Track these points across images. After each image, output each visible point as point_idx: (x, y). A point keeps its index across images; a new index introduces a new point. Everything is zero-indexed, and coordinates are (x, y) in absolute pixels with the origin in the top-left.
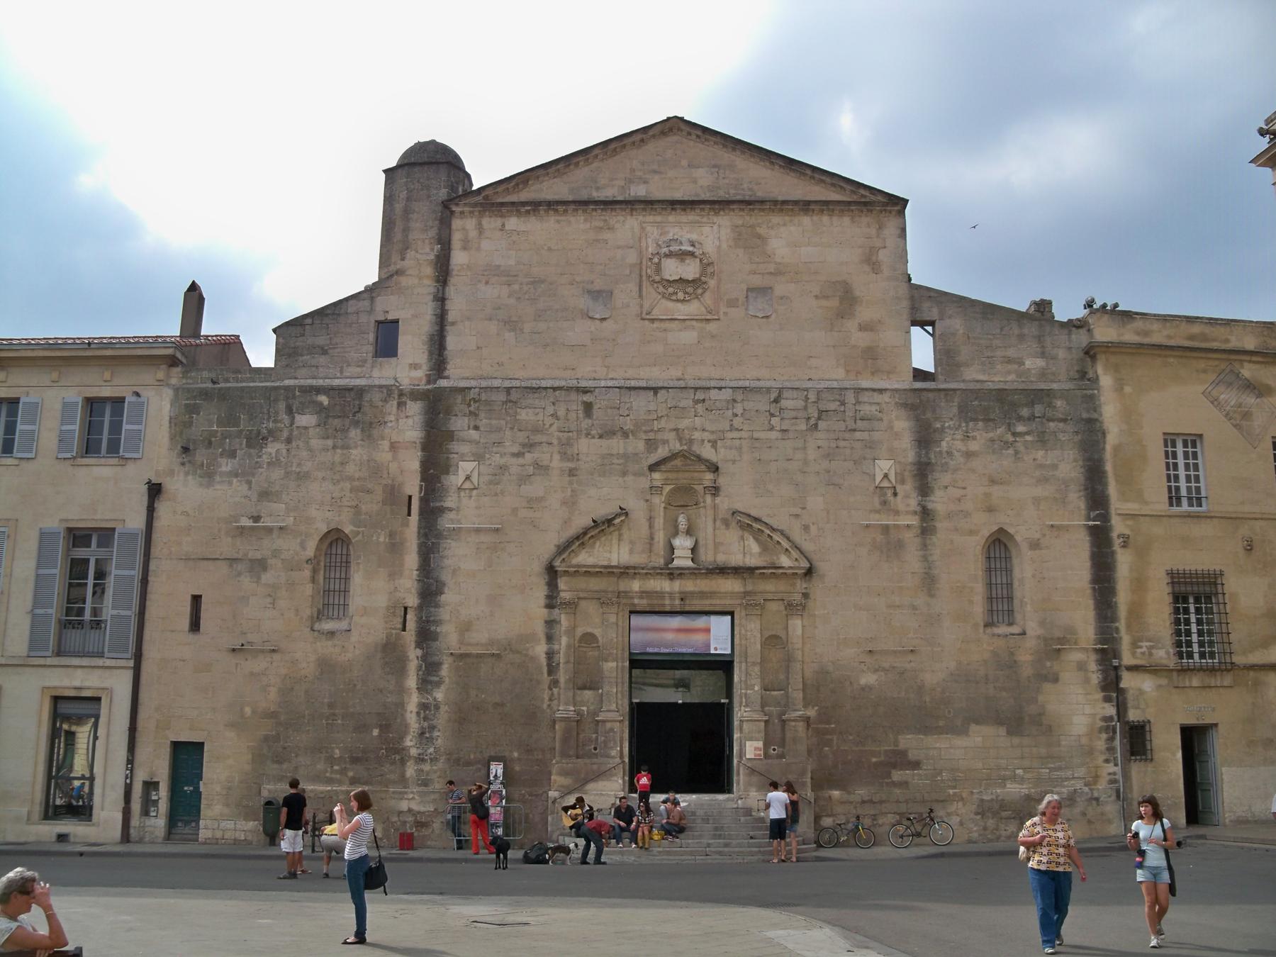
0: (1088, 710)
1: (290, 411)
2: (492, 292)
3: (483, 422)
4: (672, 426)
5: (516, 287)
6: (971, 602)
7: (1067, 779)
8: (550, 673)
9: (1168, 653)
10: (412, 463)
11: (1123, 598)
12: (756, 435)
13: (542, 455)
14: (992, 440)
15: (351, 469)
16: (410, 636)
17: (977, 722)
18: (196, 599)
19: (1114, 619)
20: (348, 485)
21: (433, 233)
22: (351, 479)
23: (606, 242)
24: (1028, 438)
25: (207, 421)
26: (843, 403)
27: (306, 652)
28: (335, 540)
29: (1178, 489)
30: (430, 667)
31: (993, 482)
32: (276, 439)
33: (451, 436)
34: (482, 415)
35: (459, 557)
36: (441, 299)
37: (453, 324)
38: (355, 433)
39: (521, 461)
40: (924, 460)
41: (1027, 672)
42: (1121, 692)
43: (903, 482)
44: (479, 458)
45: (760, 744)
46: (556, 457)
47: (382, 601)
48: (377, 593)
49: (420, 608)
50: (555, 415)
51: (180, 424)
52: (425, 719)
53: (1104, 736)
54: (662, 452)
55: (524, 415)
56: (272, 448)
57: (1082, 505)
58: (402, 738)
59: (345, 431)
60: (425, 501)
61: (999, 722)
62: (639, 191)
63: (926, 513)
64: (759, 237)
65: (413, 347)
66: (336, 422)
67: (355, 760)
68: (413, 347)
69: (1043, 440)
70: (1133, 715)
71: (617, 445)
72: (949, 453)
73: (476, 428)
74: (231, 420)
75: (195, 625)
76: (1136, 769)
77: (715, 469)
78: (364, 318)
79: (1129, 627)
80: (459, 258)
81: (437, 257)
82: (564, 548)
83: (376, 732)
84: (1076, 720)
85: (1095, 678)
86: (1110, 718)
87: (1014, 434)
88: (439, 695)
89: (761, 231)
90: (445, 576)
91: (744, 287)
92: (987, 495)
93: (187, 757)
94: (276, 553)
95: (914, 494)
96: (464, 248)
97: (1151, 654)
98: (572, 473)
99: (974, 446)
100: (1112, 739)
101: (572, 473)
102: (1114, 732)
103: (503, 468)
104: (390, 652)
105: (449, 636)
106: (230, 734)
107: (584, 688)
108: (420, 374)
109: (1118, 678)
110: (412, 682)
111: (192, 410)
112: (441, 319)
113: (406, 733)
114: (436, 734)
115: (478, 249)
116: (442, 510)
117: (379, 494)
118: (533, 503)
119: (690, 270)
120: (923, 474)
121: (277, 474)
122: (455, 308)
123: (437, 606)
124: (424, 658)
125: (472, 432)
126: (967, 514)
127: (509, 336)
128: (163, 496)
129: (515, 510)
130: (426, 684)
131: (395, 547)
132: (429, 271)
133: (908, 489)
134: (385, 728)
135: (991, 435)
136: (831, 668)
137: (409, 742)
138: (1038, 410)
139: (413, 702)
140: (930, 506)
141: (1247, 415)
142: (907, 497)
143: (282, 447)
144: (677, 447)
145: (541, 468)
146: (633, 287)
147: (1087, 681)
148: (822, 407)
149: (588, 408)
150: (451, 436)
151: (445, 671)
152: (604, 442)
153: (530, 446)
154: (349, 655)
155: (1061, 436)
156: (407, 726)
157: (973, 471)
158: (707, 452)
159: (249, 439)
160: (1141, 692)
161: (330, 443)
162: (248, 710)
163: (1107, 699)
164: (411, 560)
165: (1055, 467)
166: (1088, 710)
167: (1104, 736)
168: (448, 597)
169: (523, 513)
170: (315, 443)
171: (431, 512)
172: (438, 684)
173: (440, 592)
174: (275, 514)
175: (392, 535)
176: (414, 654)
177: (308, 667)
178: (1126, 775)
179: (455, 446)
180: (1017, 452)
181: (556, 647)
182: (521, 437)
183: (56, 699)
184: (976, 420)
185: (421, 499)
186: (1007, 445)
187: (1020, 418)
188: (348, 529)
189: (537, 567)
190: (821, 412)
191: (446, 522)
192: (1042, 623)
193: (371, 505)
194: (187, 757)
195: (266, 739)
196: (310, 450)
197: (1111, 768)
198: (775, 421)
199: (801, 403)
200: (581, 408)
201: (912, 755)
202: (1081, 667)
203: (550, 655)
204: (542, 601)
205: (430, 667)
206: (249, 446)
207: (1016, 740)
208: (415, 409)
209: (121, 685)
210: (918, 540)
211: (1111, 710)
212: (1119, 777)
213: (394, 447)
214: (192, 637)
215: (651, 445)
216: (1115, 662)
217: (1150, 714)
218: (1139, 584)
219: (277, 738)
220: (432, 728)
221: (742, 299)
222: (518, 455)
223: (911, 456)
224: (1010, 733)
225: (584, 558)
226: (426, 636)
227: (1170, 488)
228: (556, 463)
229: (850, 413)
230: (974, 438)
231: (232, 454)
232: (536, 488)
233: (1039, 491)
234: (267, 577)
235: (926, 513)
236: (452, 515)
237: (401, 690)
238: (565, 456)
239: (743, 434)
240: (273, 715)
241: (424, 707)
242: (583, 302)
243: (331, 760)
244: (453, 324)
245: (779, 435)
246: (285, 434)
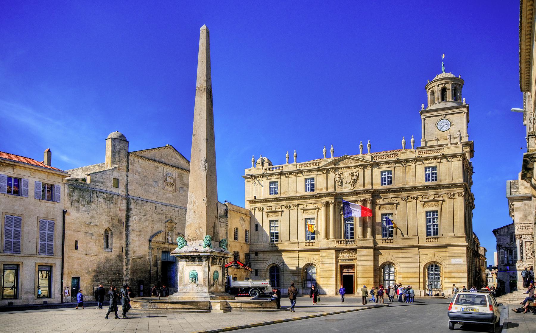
2: (136, 177)
10: (124, 214)
13: (148, 217)
16: (124, 254)
18: (77, 242)
20: (111, 217)
21: (126, 159)
25: (76, 195)
27: (103, 255)
28: (108, 230)
30: (128, 261)
35: (133, 236)
38: (112, 205)
44: (136, 215)
47: (118, 245)
48: (116, 243)
54: (167, 219)
55: (145, 207)
60: (127, 223)
62: (163, 160)
65: (122, 187)
66: (108, 202)
67: (113, 281)
68: (122, 187)
71: (160, 216)
77: (176, 224)
78: (111, 177)
80: (130, 167)
82: (152, 236)
88: (129, 266)
90: (130, 241)
93: (76, 280)
98: (153, 221)
101: (153, 221)
104: (120, 257)
106: (87, 275)
108: (124, 193)
110: (124, 264)
119: (172, 181)
124: (127, 258)
127: (140, 188)
128: (66, 214)
130: (127, 264)
131: (121, 233)
134: (119, 274)
137: (124, 277)
139: (125, 269)
143: (96, 206)
144: (170, 218)
146: (162, 182)
150: (131, 209)
151: (130, 262)
158: (174, 220)
161: (106, 207)
162: (90, 269)
164: (124, 236)
168: (131, 246)
170: (104, 206)
171: (127, 226)
174: (94, 222)
175: (120, 230)
176: (125, 257)
177: (103, 260)
179: (131, 212)
188: (111, 228)
189: (147, 241)
191: (130, 228)
193: (116, 222)
194: (76, 280)
195: (94, 276)
205: (128, 261)
206: (88, 204)
208: (124, 201)
209: (58, 262)
214: (76, 251)
215: (166, 217)
219: (97, 276)
225: (155, 239)
232: (146, 224)
234: (94, 237)
237: (123, 266)
240: (95, 270)
241: (127, 269)
242: (153, 183)
243: (108, 281)
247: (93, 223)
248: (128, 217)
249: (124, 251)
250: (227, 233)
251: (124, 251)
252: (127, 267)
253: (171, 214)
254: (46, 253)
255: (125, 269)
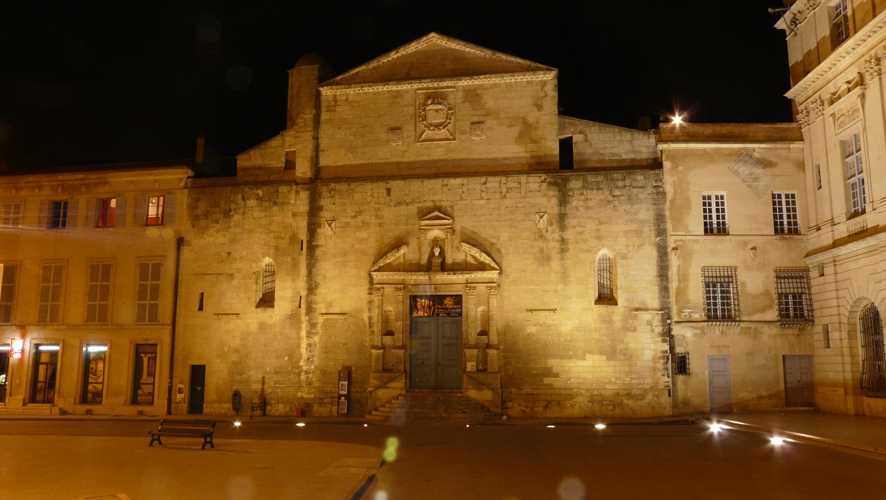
0: (652, 347)
1: (244, 199)
3: (338, 201)
4: (431, 199)
5: (353, 130)
6: (587, 288)
7: (641, 384)
8: (370, 327)
9: (701, 315)
11: (674, 285)
12: (474, 202)
14: (601, 200)
15: (273, 228)
17: (591, 352)
19: (668, 298)
22: (273, 232)
23: (398, 103)
24: (622, 198)
26: (520, 183)
29: (711, 224)
31: (600, 223)
32: (237, 213)
33: (321, 208)
34: (337, 197)
36: (316, 138)
37: (323, 151)
38: (275, 208)
39: (355, 220)
40: (563, 212)
41: (618, 325)
42: (672, 337)
43: (551, 224)
45: (474, 363)
46: (373, 218)
49: (308, 296)
50: (372, 196)
51: (192, 207)
52: (310, 351)
53: (662, 361)
56: (236, 218)
57: (653, 234)
58: (299, 361)
59: (270, 208)
60: (310, 242)
61: (601, 353)
63: (563, 241)
64: (477, 95)
66: (267, 204)
69: (630, 200)
70: (679, 350)
71: (403, 210)
72: (577, 207)
73: (334, 204)
74: (217, 205)
75: (201, 308)
76: (681, 378)
79: (677, 301)
80: (324, 116)
81: (314, 116)
83: (286, 359)
84: (646, 352)
85: (659, 329)
86: (666, 352)
87: (613, 196)
88: (316, 339)
89: (479, 92)
90: (319, 279)
91: (469, 123)
92: (598, 230)
94: (238, 270)
95: (557, 230)
96: (327, 111)
97: (690, 316)
99: (591, 204)
100: (667, 363)
101: (380, 225)
102: (668, 359)
103: (347, 224)
104: (294, 318)
105: (321, 308)
107: (385, 335)
109: (670, 330)
110: (303, 333)
111: (198, 200)
112: (317, 148)
113: (301, 358)
114: (315, 359)
115: (335, 111)
116: (317, 246)
117: (287, 240)
118: (361, 241)
120: (562, 218)
121: (239, 230)
122: (324, 142)
123: (316, 295)
124: (309, 321)
125: (332, 206)
126: (585, 241)
129: (353, 246)
130: (309, 334)
131: (295, 264)
132: (310, 123)
133: (555, 226)
134: (291, 356)
135: (600, 197)
136: (511, 324)
137: (302, 363)
138: (627, 182)
139: (304, 345)
140: (565, 237)
141: (756, 179)
142: (553, 232)
143: (240, 217)
145: (365, 224)
147: (653, 331)
148: (509, 185)
149: (389, 191)
150: (321, 208)
151: (319, 328)
152: (397, 209)
153: (360, 212)
154: (274, 320)
155: (640, 196)
156: (300, 354)
157: (590, 218)
159: (224, 213)
160: (684, 337)
161: (263, 214)
163: (664, 341)
164: (303, 271)
165: (636, 213)
166: (652, 347)
167: (662, 361)
168: (321, 290)
169: (357, 246)
170: (257, 214)
171: (312, 248)
172: (316, 334)
173: (317, 287)
175: (294, 259)
176: (304, 318)
178: (674, 384)
180: (615, 206)
181: (373, 314)
182: (356, 208)
183: (138, 345)
184: (592, 189)
185: (308, 241)
186: (609, 202)
187: (618, 188)
189: (364, 274)
190: (507, 189)
191: (318, 252)
192: (627, 300)
196: (254, 218)
197: (666, 379)
198: (483, 194)
199: (497, 185)
200: (385, 191)
201: (555, 370)
202: (649, 323)
203: (370, 318)
204: (366, 292)
205: (313, 325)
207: (612, 363)
210: (558, 255)
211: (666, 347)
212: (670, 384)
213: (294, 215)
214: (200, 313)
216: (669, 321)
217: (689, 349)
218: (683, 278)
220: (313, 356)
221: (468, 129)
222: (355, 217)
223: (556, 210)
224: (608, 359)
226: (310, 310)
227: (705, 224)
228: (373, 219)
229: (523, 189)
230: (591, 199)
231: (217, 222)
232: (363, 234)
233: (625, 228)
235: (563, 241)
236: (323, 249)
237: (299, 338)
238: (377, 216)
239: (467, 202)
241: (309, 345)
244: (323, 151)
245: (486, 201)
246: (242, 210)
247: (234, 254)
248: (313, 229)
249: (303, 306)
250: (660, 219)
251: (303, 306)
252: (311, 341)
253: (436, 198)
254: (147, 322)
255: (304, 345)
